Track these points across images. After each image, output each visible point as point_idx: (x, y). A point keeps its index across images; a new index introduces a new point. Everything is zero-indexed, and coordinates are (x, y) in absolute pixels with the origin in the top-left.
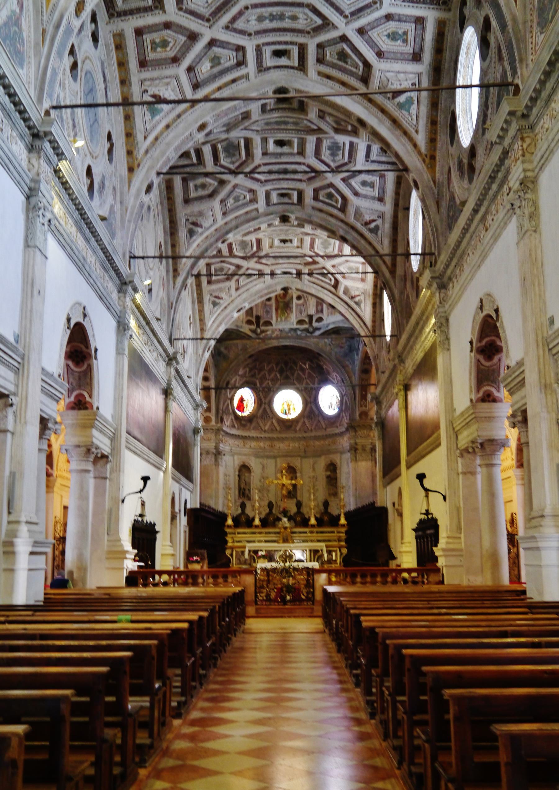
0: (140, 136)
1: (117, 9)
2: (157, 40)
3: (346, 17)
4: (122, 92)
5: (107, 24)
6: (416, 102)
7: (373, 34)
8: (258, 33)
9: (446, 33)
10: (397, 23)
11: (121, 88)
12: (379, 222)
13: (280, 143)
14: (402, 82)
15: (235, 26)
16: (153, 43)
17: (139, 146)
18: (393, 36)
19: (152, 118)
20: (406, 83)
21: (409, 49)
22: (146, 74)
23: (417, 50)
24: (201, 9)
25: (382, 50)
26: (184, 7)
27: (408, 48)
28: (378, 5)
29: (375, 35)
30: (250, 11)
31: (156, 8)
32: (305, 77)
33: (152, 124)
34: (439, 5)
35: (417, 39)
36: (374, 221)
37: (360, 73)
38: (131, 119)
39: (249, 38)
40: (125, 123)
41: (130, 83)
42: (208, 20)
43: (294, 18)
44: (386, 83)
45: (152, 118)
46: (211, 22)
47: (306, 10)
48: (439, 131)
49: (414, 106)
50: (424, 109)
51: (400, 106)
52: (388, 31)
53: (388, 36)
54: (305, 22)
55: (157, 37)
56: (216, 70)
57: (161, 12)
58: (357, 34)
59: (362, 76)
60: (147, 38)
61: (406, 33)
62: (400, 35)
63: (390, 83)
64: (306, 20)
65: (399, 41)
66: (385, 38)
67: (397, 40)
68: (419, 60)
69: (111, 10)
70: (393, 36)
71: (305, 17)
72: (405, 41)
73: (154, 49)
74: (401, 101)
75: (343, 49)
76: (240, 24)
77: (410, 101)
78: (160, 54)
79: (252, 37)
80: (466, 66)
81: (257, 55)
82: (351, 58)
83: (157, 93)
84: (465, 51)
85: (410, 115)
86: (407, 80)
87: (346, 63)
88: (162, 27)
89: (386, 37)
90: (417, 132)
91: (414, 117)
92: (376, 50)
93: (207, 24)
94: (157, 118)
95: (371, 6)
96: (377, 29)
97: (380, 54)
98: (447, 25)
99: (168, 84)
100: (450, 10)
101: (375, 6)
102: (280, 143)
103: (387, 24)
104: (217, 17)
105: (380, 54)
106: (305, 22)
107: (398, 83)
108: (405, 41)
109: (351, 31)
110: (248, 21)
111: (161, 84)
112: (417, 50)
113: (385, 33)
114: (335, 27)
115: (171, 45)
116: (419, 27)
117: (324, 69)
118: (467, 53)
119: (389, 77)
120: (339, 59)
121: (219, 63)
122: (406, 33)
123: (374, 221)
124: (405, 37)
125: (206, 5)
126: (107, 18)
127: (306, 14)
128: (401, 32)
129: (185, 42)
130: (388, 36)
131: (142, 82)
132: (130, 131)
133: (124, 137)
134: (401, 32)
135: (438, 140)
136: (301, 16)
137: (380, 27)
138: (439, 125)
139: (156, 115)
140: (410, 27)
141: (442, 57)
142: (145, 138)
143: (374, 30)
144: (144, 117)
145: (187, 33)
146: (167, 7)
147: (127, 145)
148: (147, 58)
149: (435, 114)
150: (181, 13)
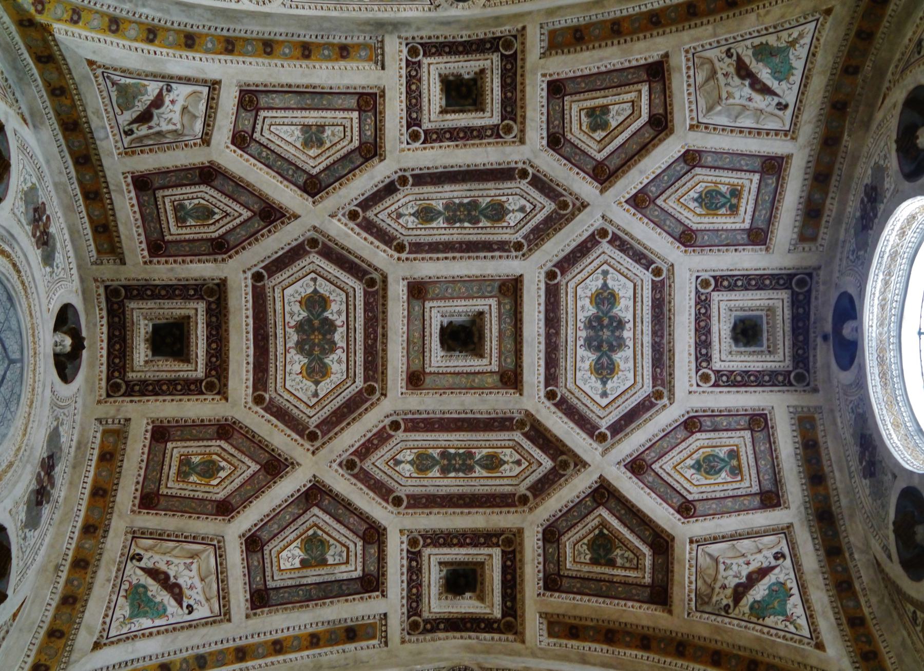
0: (84, 639)
1: (131, 375)
2: (196, 459)
3: (602, 438)
4: (79, 548)
5: (99, 402)
6: (795, 591)
7: (665, 466)
8: (417, 248)
9: (821, 440)
10: (712, 435)
11: (80, 539)
12: (784, 573)
14: (751, 558)
15: (367, 465)
16: (185, 462)
17: (74, 656)
18: (707, 466)
19: (132, 616)
20: (760, 557)
21: (749, 484)
22: (150, 521)
23: (768, 485)
24: (302, 407)
25: (690, 497)
26: (267, 396)
27: (746, 483)
28: (665, 400)
29: (668, 468)
30: (400, 435)
31: (210, 387)
32: (518, 646)
33: (125, 630)
34: (791, 385)
35: (762, 463)
36: (763, 572)
37: (648, 580)
38: (78, 606)
39: (395, 510)
40: (58, 608)
41: (106, 531)
42: (312, 437)
43: (493, 463)
44: (712, 572)
45: (132, 616)
46: (317, 444)
47: (517, 436)
48: (876, 635)
49: (795, 599)
50: (820, 598)
51: (759, 610)
52: (695, 456)
53: (698, 466)
54: (518, 470)
55: (196, 451)
56: (313, 576)
57: (218, 397)
58: (629, 474)
59: (652, 586)
60: (175, 450)
61: (734, 454)
62: (723, 460)
63: (722, 567)
64: (518, 463)
65: (723, 474)
66: (689, 473)
67: (720, 470)
68: (778, 505)
69: (116, 374)
70: (707, 466)
71: (518, 457)
72: (737, 471)
73: (182, 475)
74: (758, 598)
75: (604, 524)
76: (381, 215)
77: (780, 592)
78: (195, 486)
79: (401, 509)
80: (892, 402)
81: (410, 581)
82: (625, 544)
83: (163, 567)
84: (876, 371)
85: (789, 619)
86: (760, 551)
87: (612, 563)
88: (211, 430)
89: (693, 471)
90: (820, 646)
91: (803, 622)
92: (677, 501)
93: (307, 445)
94: (146, 622)
95: (653, 405)
96: (671, 454)
97: (686, 509)
98: (819, 422)
99: (194, 555)
100: (815, 390)
101: (661, 403)
103: (691, 440)
104: (332, 434)
105: (686, 509)
106: (518, 470)
107: (741, 561)
108: (737, 471)
109: (614, 469)
110: (398, 463)
111: (175, 552)
112: (768, 485)
113: (690, 462)
114: (580, 464)
115: (222, 474)
116: (760, 435)
117: (561, 602)
118: (883, 375)
119: (716, 554)
120: (595, 561)
121: (323, 562)
122: (734, 454)
123: (763, 572)
124: (734, 462)
125: (314, 400)
126: (103, 392)
127: (517, 447)
128: (722, 453)
129: (255, 473)
130: (698, 466)
131: (136, 535)
132: (64, 628)
133: (42, 632)
134: (722, 453)
135: (884, 651)
136: (508, 455)
137: (677, 449)
138: (871, 623)
139: (145, 615)
140: (742, 440)
141: (826, 488)
142: (97, 646)
143: (665, 459)
144: (111, 608)
145: (265, 457)
146: (231, 384)
147: (40, 652)
148: (163, 491)
149: (851, 604)
150: (258, 409)
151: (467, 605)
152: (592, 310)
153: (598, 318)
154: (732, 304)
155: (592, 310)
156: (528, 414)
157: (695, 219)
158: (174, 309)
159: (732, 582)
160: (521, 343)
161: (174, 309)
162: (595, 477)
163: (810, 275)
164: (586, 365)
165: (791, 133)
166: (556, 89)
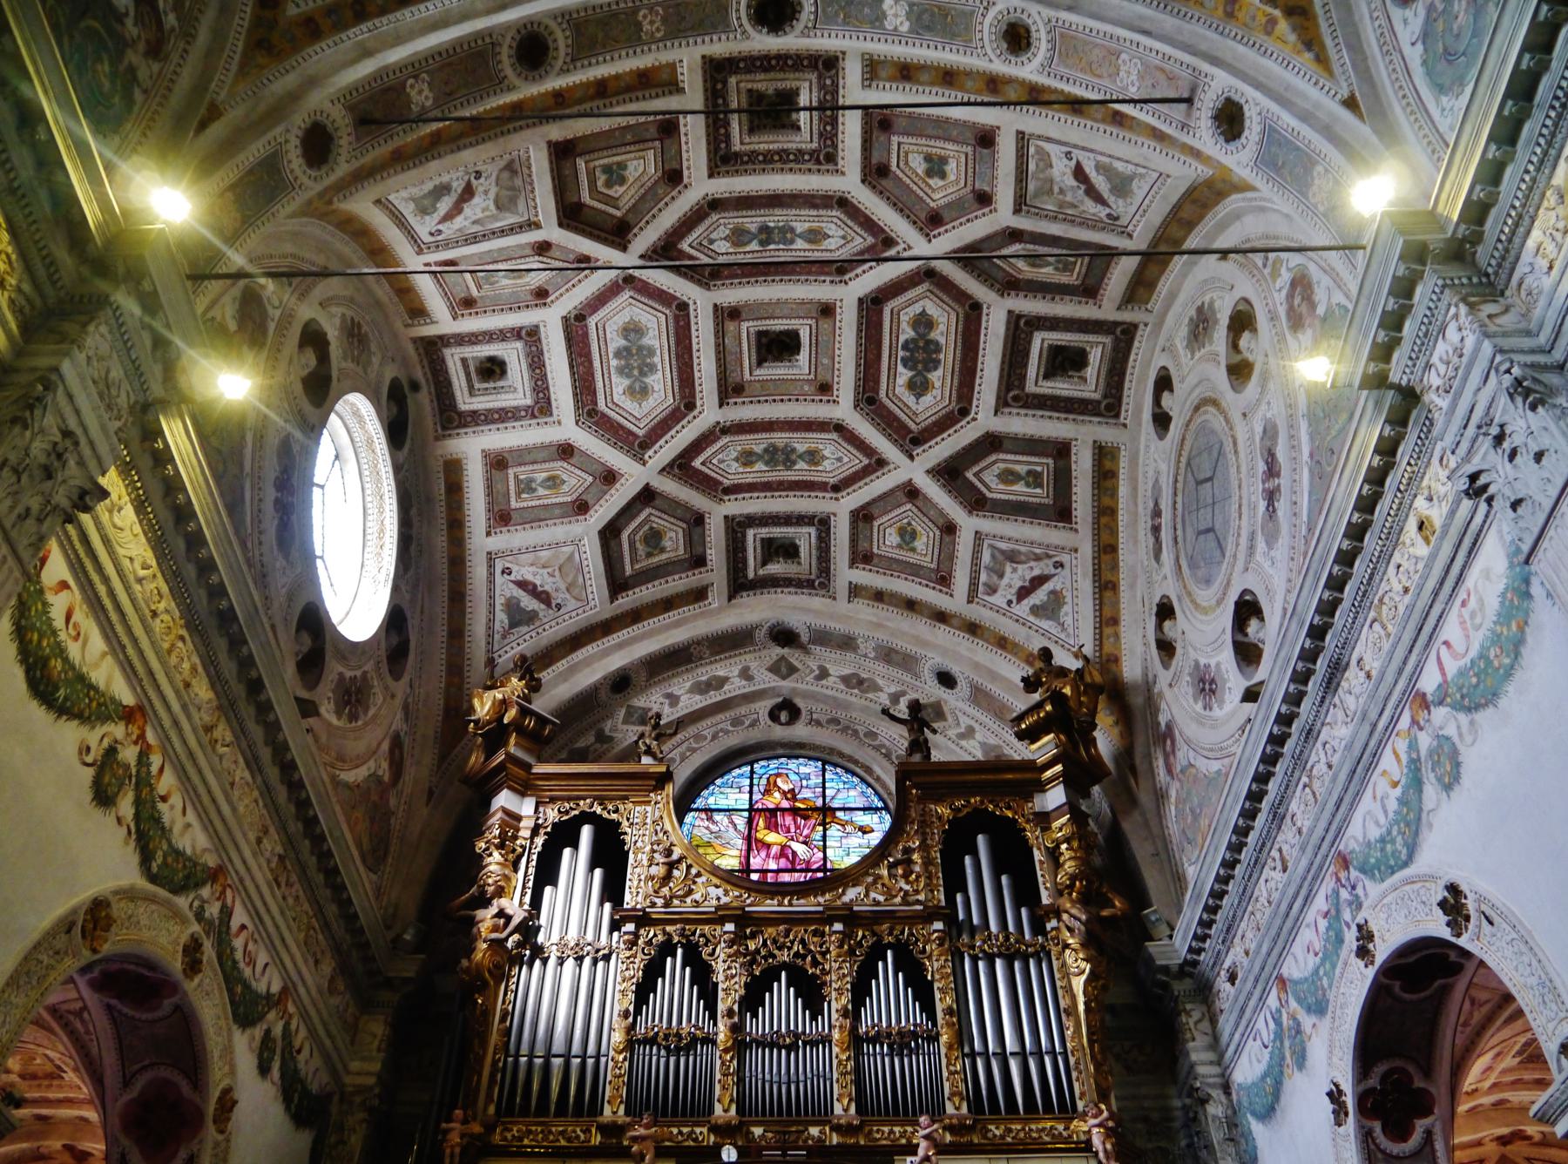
13: (789, 551)
102: (789, 551)
151: (766, 84)
152: (649, 380)
153: (643, 374)
154: (511, 396)
155: (649, 380)
156: (707, 287)
157: (560, 468)
158: (1061, 387)
159: (476, 200)
160: (717, 345)
161: (1061, 387)
162: (631, 247)
163: (444, 428)
164: (651, 333)
165: (491, 558)
166: (699, 561)
